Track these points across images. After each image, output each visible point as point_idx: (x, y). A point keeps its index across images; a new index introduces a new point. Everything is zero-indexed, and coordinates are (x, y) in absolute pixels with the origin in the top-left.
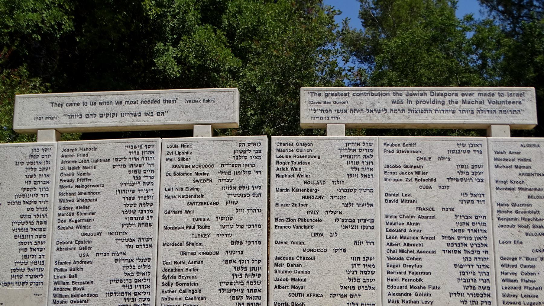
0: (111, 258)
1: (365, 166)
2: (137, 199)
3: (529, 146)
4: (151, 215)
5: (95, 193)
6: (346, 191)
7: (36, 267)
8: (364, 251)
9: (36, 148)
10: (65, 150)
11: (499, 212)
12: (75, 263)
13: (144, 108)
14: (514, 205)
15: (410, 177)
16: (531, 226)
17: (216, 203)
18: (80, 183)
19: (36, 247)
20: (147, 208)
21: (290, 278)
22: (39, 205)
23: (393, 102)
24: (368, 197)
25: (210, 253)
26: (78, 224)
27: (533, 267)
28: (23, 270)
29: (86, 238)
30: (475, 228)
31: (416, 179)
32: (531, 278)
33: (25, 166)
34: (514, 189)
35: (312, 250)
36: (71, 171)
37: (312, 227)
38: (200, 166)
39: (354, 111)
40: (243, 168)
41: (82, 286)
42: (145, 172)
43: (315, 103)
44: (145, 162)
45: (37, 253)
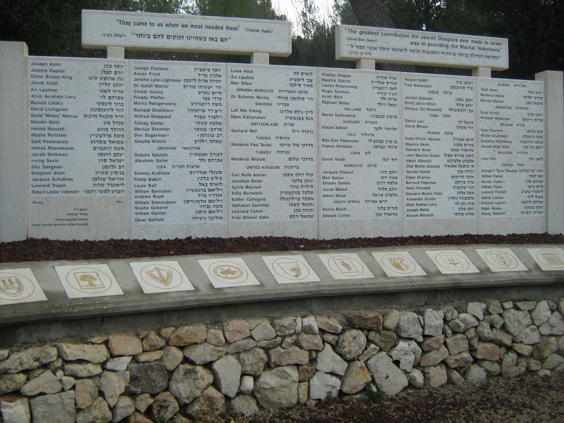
0: (187, 170)
1: (391, 97)
2: (207, 118)
3: (503, 85)
4: (220, 133)
5: (168, 111)
6: (377, 117)
7: (116, 176)
8: (391, 166)
9: (108, 64)
10: (137, 68)
11: (482, 135)
12: (153, 173)
14: (492, 130)
15: (423, 107)
16: (502, 147)
17: (276, 125)
18: (153, 100)
19: (115, 158)
20: (216, 126)
21: (334, 189)
22: (115, 119)
23: (412, 43)
24: (393, 123)
25: (271, 168)
26: (154, 138)
27: (501, 176)
28: (104, 179)
29: (163, 152)
30: (466, 148)
31: (428, 109)
32: (500, 185)
33: (98, 80)
34: (492, 118)
35: (351, 165)
36: (144, 89)
37: (351, 147)
38: (261, 90)
39: (383, 49)
40: (296, 95)
41: (161, 194)
42: (213, 93)
43: (352, 39)
44: (214, 84)
45: (117, 164)
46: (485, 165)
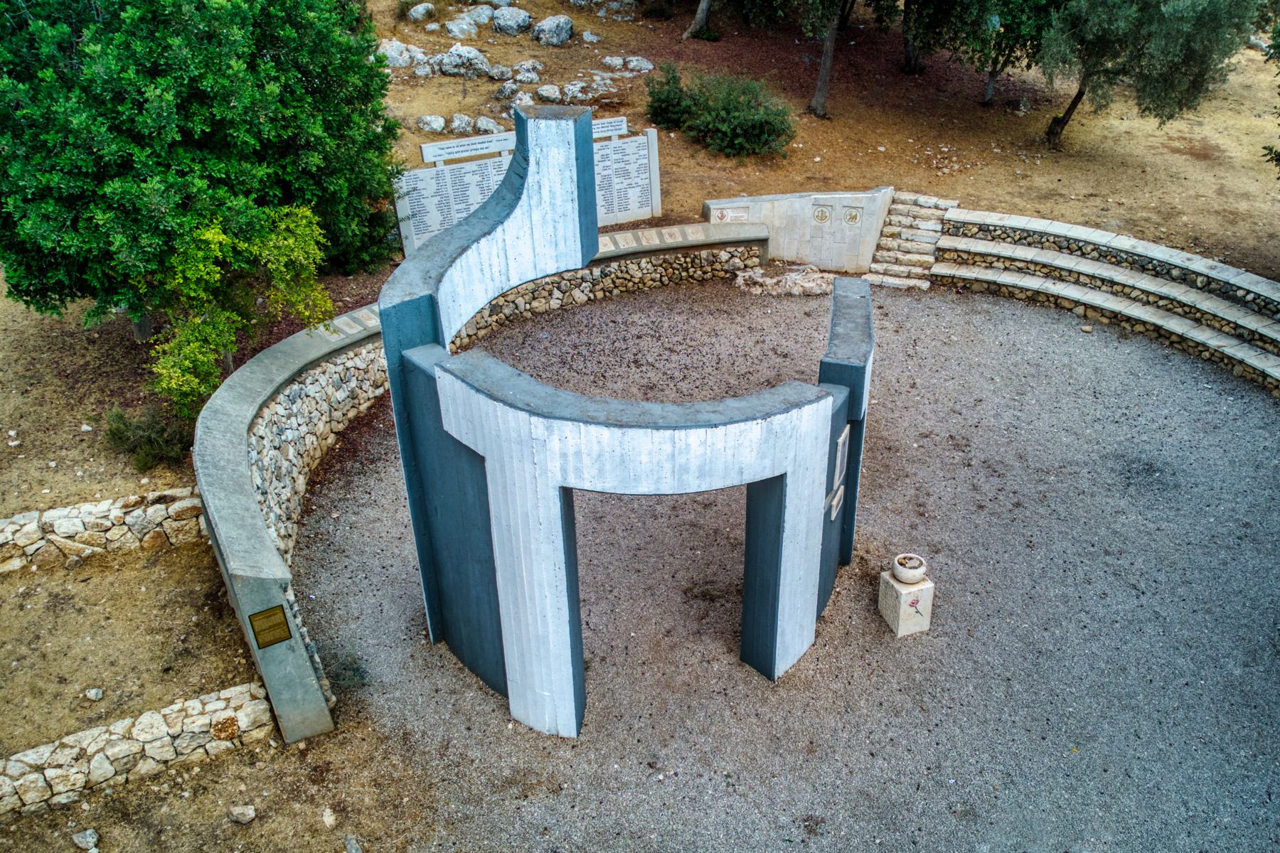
13: (479, 146)
46: (618, 187)
